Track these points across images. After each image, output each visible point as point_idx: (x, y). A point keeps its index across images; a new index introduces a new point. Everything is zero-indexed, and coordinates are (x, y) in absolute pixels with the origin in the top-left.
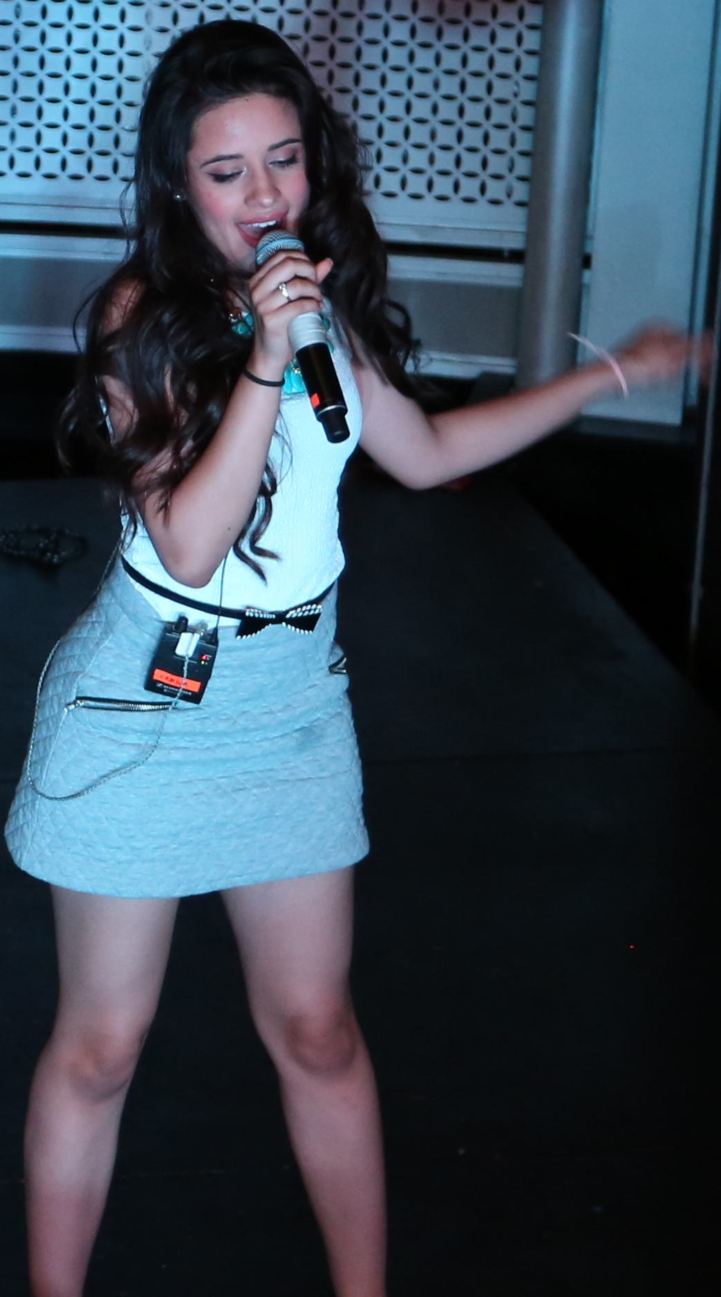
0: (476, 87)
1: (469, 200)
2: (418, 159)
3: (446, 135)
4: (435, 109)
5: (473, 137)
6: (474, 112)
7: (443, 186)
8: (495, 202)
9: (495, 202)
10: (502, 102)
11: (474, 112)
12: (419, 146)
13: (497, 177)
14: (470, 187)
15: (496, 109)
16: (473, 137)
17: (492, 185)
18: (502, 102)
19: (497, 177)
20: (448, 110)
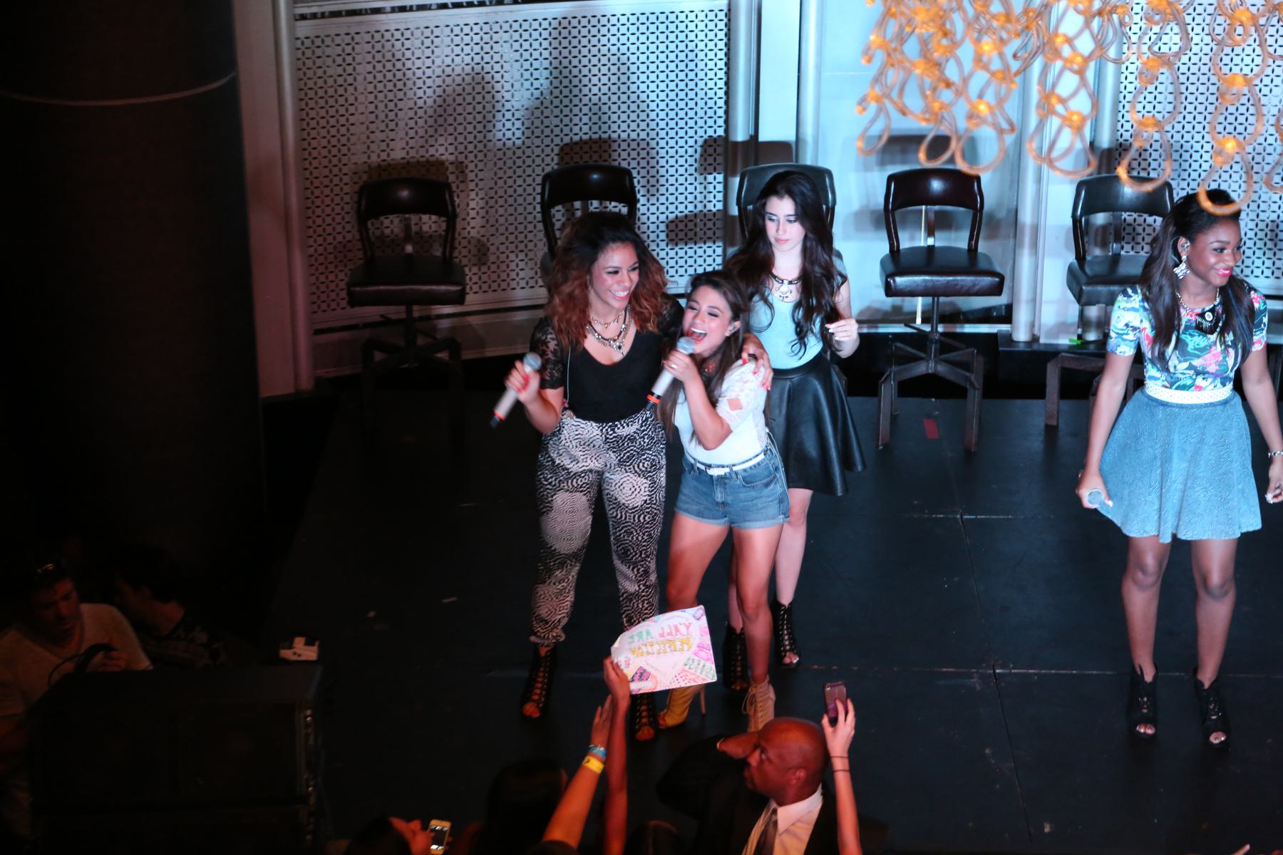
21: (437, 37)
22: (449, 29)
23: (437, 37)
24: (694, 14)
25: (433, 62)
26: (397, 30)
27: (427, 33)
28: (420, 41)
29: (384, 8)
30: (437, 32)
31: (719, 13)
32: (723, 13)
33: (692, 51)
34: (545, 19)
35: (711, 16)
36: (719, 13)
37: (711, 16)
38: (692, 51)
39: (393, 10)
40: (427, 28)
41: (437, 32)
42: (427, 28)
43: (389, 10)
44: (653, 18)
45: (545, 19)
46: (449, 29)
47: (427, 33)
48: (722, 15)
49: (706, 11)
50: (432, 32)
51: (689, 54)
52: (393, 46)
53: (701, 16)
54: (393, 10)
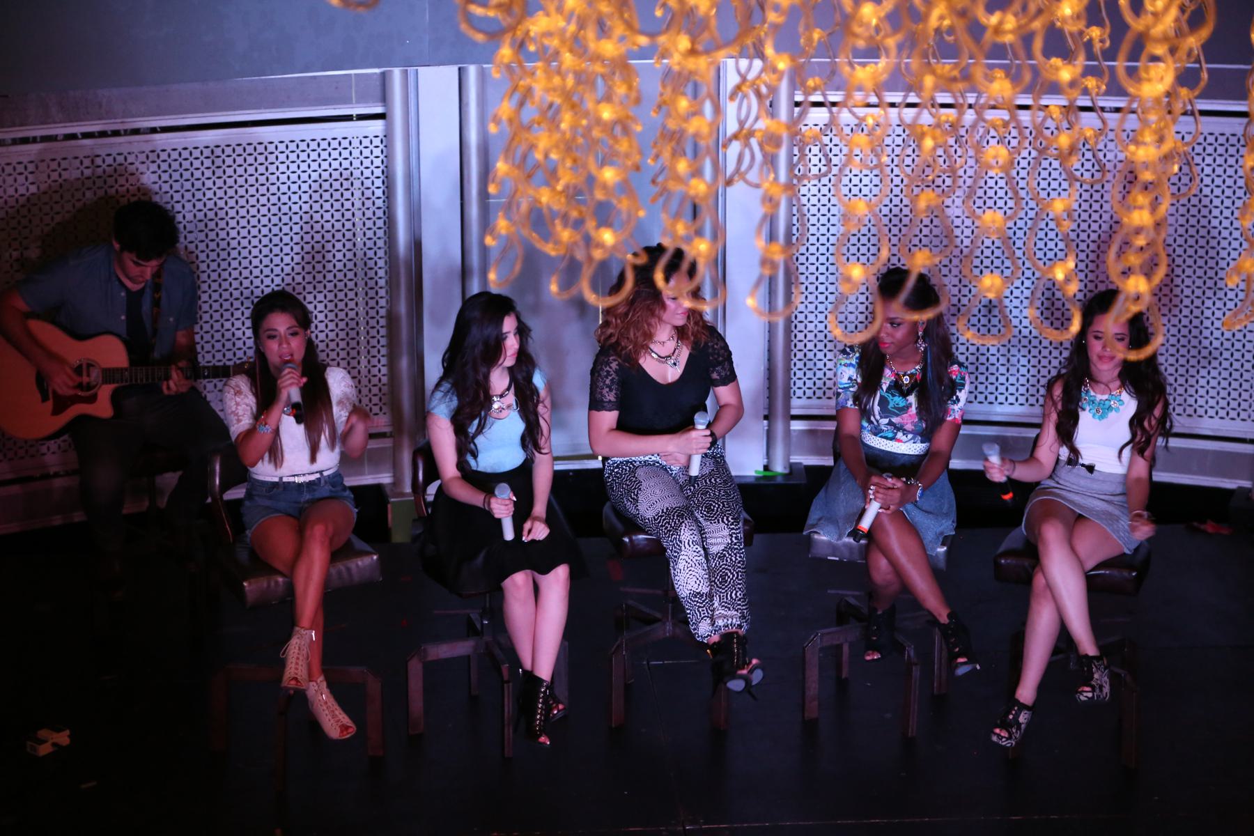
0: (1236, 375)
1: (1233, 419)
2: (1212, 402)
3: (1223, 394)
4: (1219, 383)
5: (1234, 394)
6: (1235, 385)
7: (1222, 413)
8: (1243, 420)
9: (1243, 420)
10: (1246, 381)
11: (1235, 385)
12: (1212, 398)
13: (1244, 410)
14: (1233, 414)
15: (1244, 383)
16: (1234, 394)
17: (1242, 413)
18: (1246, 381)
19: (1244, 410)
20: (1224, 384)
21: (65, 170)
22: (78, 161)
23: (65, 170)
24: (347, 141)
25: (62, 197)
26: (20, 163)
27: (54, 165)
28: (45, 175)
29: (4, 140)
30: (64, 164)
31: (374, 139)
32: (379, 139)
33: (347, 179)
34: (185, 149)
35: (366, 142)
36: (374, 139)
37: (366, 142)
38: (347, 179)
39: (15, 142)
40: (53, 160)
41: (64, 164)
42: (53, 160)
43: (10, 142)
44: (303, 146)
45: (185, 149)
46: (78, 161)
47: (54, 165)
48: (377, 142)
49: (361, 138)
50: (59, 165)
51: (344, 182)
52: (15, 180)
53: (356, 143)
54: (15, 142)
